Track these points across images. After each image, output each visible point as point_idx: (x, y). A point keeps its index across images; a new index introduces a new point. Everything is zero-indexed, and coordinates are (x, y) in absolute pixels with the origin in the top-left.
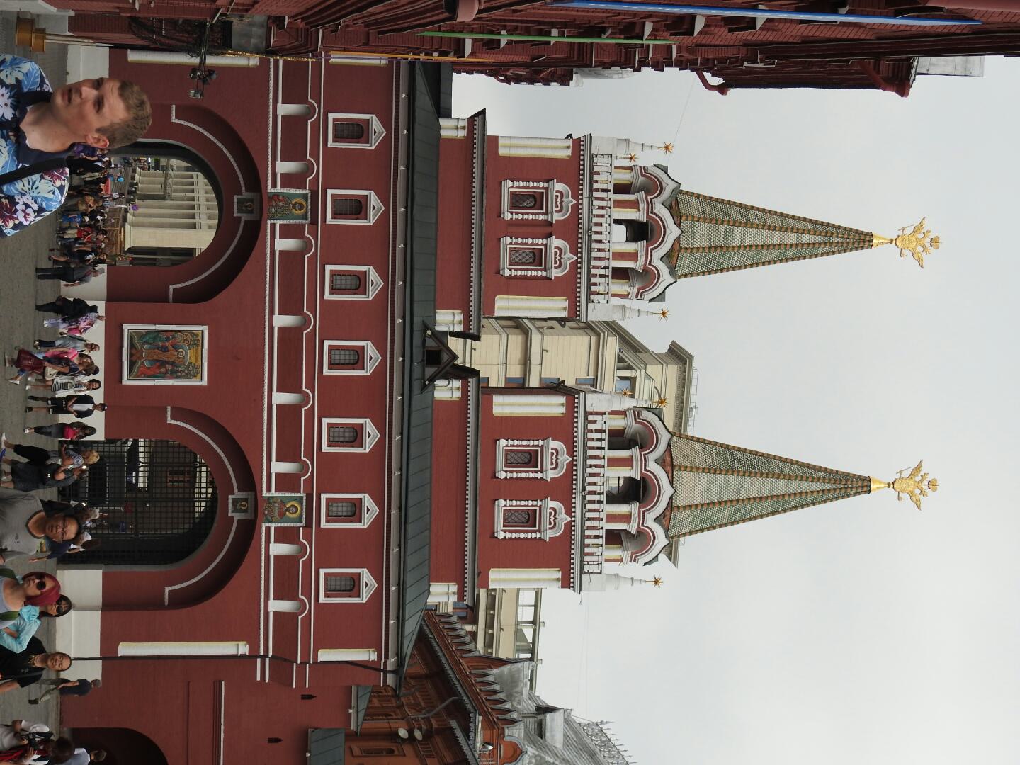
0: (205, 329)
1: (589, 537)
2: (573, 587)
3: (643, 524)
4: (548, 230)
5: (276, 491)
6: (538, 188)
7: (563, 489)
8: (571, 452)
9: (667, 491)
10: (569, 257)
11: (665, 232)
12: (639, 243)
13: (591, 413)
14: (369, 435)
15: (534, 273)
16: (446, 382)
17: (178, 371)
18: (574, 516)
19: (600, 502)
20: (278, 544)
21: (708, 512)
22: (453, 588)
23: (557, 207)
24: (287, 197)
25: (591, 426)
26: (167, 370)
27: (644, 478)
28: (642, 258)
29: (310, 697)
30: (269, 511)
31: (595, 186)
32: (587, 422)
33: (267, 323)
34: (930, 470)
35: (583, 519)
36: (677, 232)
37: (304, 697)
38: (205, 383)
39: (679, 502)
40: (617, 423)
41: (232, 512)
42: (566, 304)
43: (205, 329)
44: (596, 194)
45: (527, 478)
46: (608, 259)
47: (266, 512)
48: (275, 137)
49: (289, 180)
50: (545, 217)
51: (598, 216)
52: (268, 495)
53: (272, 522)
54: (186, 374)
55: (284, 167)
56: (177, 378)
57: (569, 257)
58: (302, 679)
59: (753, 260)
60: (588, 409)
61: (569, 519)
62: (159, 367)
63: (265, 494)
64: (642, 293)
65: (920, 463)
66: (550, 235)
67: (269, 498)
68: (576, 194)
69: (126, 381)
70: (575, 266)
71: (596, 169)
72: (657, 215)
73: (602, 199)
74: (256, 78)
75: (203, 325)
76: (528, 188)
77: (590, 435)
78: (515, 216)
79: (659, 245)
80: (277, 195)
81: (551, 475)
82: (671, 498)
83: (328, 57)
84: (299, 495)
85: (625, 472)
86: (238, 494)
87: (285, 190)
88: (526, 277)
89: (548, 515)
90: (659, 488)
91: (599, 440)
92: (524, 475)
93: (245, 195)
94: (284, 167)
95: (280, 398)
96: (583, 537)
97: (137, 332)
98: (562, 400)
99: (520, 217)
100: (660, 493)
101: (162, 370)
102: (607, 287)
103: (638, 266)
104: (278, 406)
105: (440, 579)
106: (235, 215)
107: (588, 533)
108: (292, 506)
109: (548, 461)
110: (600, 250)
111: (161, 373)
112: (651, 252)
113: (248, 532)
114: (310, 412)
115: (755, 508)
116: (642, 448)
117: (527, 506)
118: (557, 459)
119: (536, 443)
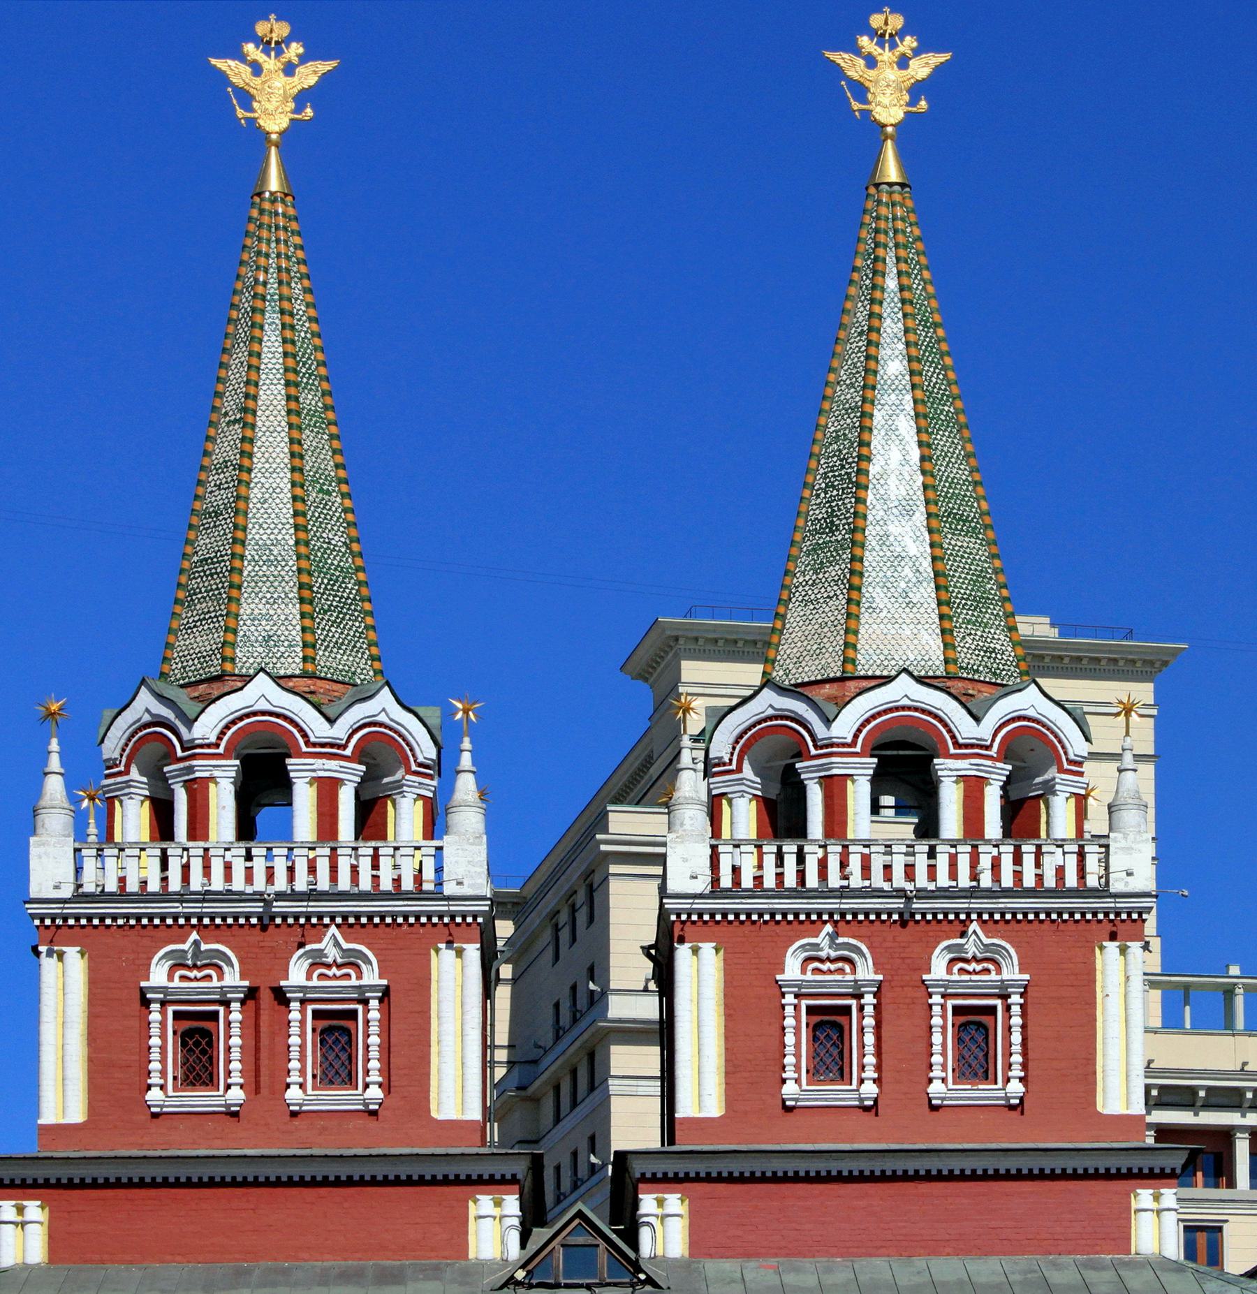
1: (1018, 875)
2: (1140, 914)
3: (988, 748)
4: (266, 997)
6: (163, 1024)
9: (903, 690)
11: (264, 713)
12: (292, 774)
13: (715, 881)
18: (968, 915)
19: (932, 854)
23: (209, 977)
25: (747, 882)
27: (875, 748)
28: (329, 767)
31: (154, 886)
36: (262, 684)
40: (743, 817)
44: (175, 885)
46: (334, 849)
51: (228, 877)
59: (328, 493)
61: (974, 926)
64: (420, 765)
66: (281, 997)
71: (112, 886)
72: (223, 733)
73: (186, 868)
76: (163, 1049)
77: (769, 882)
78: (236, 1078)
79: (296, 725)
82: (920, 680)
85: (859, 794)
89: (966, 977)
90: (897, 709)
91: (780, 861)
98: (683, 953)
99: (236, 1065)
100: (909, 708)
102: (402, 851)
103: (350, 775)
105: (1122, 1239)
107: (1007, 881)
110: (312, 869)
112: (314, 745)
116: (801, 754)
118: (829, 959)
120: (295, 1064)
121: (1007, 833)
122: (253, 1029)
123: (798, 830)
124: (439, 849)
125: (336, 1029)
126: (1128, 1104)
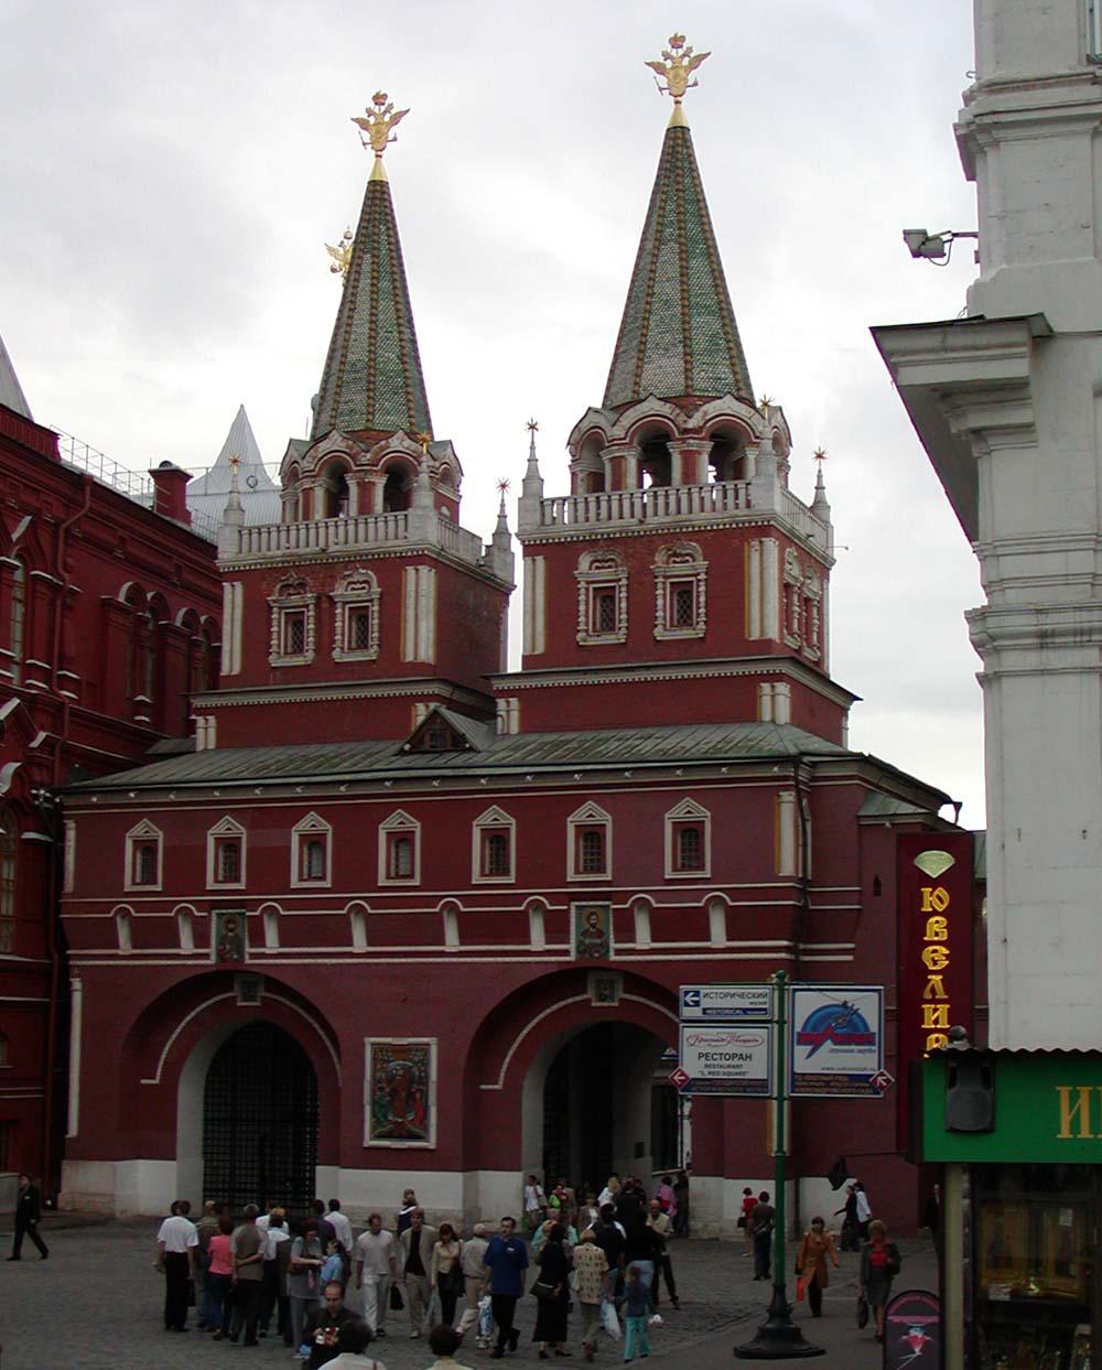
5: (568, 943)
9: (652, 406)
14: (496, 819)
16: (499, 719)
17: (420, 1077)
20: (532, 939)
21: (700, 343)
24: (222, 941)
26: (418, 1090)
30: (596, 952)
33: (454, 960)
34: (657, 49)
37: (877, 893)
39: (677, 385)
41: (613, 1001)
45: (628, 598)
47: (596, 955)
48: (156, 957)
49: (201, 939)
50: (311, 607)
52: (573, 953)
53: (605, 946)
54: (423, 1064)
55: (187, 944)
56: (427, 1076)
62: (414, 1099)
66: (331, 598)
67: (578, 952)
69: (431, 1143)
80: (220, 953)
84: (573, 912)
87: (213, 942)
92: (624, 605)
93: (236, 992)
94: (187, 944)
95: (452, 941)
97: (374, 1128)
101: (418, 1096)
103: (380, 482)
104: (654, 939)
109: (606, 574)
111: (421, 1098)
114: (466, 900)
117: (664, 595)
119: (583, 591)
122: (318, 618)
123: (602, 490)
124: (406, 516)
125: (360, 615)
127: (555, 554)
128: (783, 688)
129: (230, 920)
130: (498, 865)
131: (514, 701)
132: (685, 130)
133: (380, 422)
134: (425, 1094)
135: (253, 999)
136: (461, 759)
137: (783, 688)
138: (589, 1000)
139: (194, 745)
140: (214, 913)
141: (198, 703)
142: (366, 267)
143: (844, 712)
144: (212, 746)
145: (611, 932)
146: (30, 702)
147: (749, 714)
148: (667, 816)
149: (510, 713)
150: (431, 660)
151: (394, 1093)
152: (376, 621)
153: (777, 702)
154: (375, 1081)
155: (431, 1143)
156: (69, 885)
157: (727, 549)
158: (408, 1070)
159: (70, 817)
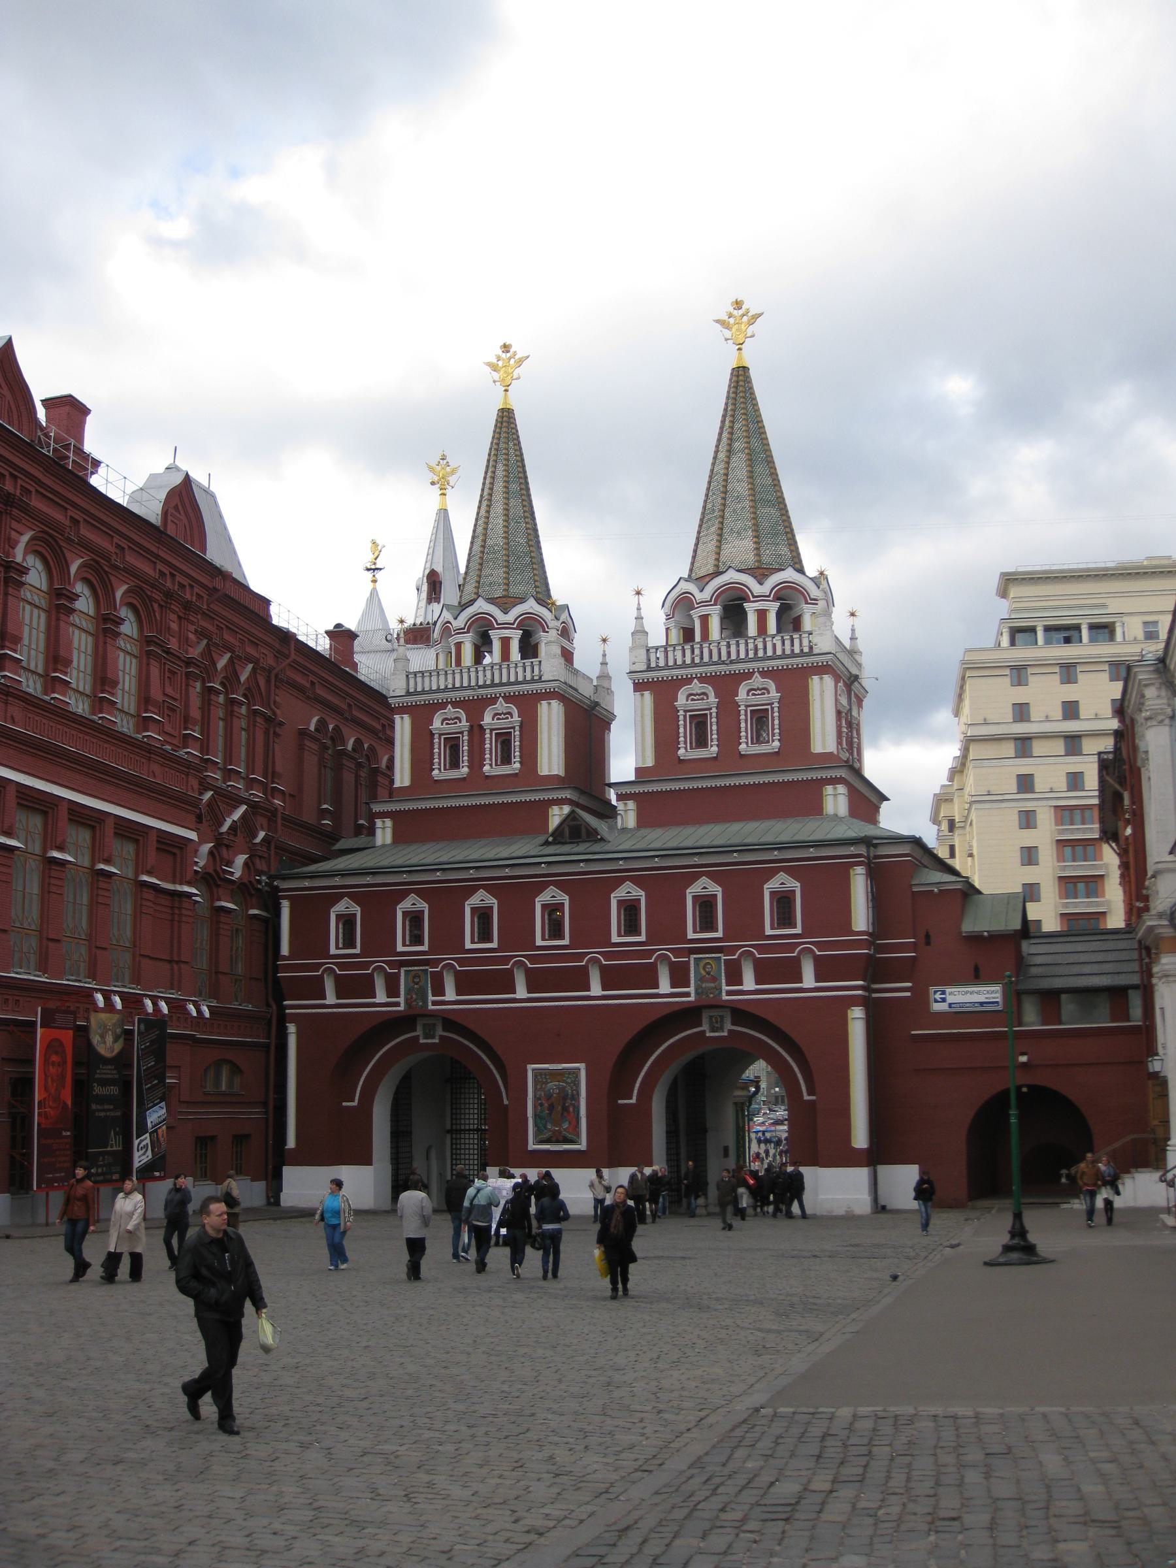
0: (530, 1067)
4: (476, 728)
7: (726, 684)
8: (688, 680)
9: (732, 576)
10: (501, 706)
15: (517, 739)
16: (619, 818)
17: (573, 1095)
22: (829, 789)
24: (409, 991)
28: (506, 633)
29: (927, 936)
32: (658, 668)
34: (723, 309)
35: (756, 659)
37: (928, 943)
38: (582, 1066)
39: (750, 559)
42: (544, 703)
43: (530, 1067)
48: (355, 1006)
49: (392, 991)
50: (466, 733)
52: (693, 995)
55: (381, 997)
56: (578, 1094)
57: (501, 706)
58: (902, 947)
60: (644, 667)
62: (569, 1112)
63: (692, 998)
65: (717, 321)
66: (482, 729)
67: (697, 993)
68: (442, 705)
69: (583, 1146)
70: (508, 698)
74: (312, 1027)
75: (526, 1071)
80: (406, 1000)
81: (713, 699)
82: (738, 571)
83: (285, 958)
84: (692, 962)
86: (705, 1027)
88: (521, 747)
92: (714, 727)
93: (419, 1032)
94: (381, 997)
96: (784, 656)
97: (535, 1136)
103: (516, 636)
106: (437, 1041)
108: (704, 968)
113: (740, 1014)
114: (606, 955)
115: (764, 480)
119: (681, 718)
120: (487, 756)
121: (779, 630)
125: (504, 740)
126: (824, 747)
127: (658, 687)
128: (842, 789)
129: (416, 975)
130: (631, 927)
131: (631, 805)
132: (745, 369)
133: (515, 590)
134: (577, 1108)
135: (433, 1037)
136: (597, 847)
137: (842, 789)
138: (704, 1032)
139: (374, 841)
140: (403, 970)
141: (376, 808)
142: (500, 472)
143: (877, 809)
144: (389, 840)
145: (723, 978)
146: (253, 806)
147: (815, 808)
148: (766, 886)
149: (628, 815)
150: (562, 773)
151: (551, 1108)
152: (517, 743)
153: (836, 801)
154: (536, 1098)
155: (583, 1146)
156: (285, 950)
157: (793, 682)
158: (562, 1089)
159: (285, 897)
